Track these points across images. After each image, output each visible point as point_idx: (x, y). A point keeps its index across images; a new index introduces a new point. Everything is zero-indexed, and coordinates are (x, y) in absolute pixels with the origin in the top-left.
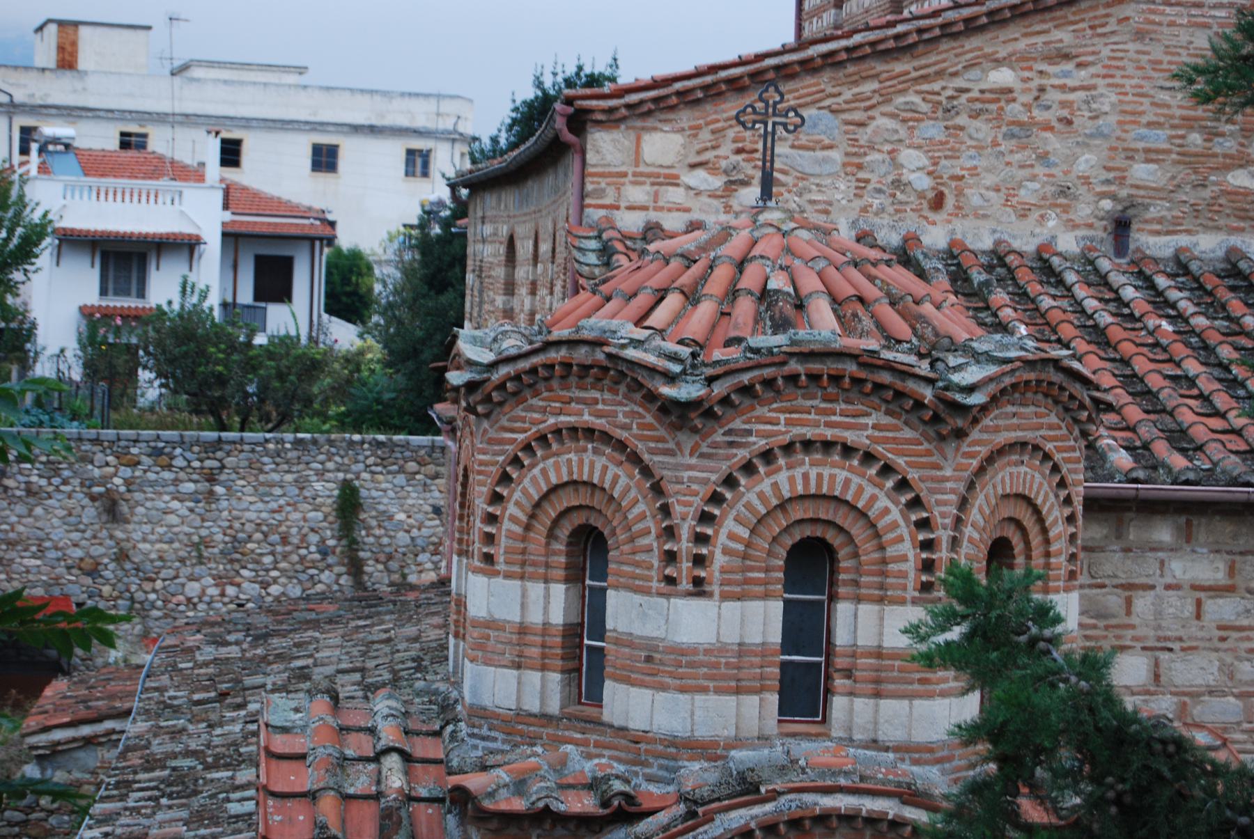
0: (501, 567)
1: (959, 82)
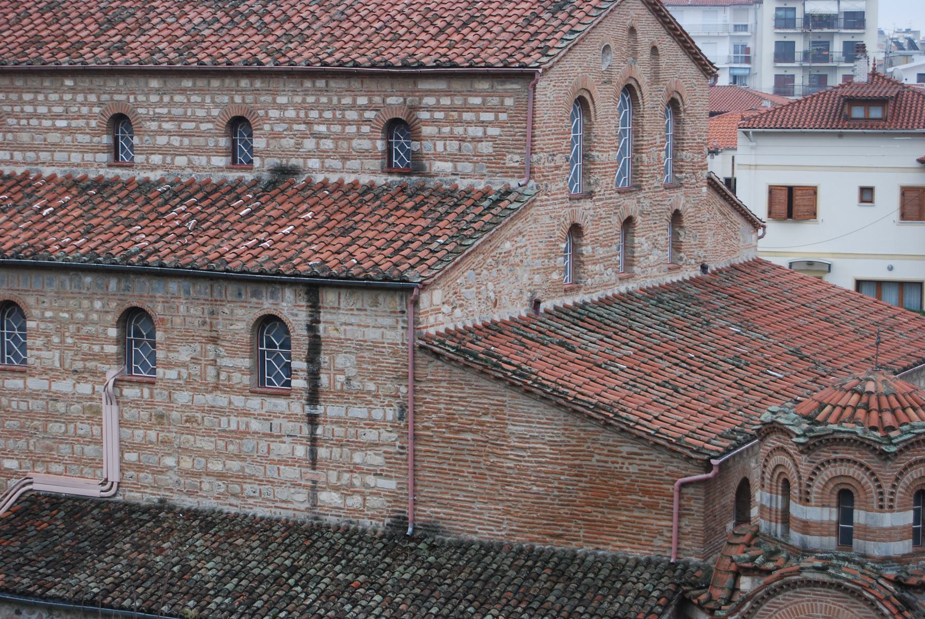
0: (896, 508)
1: (499, 251)
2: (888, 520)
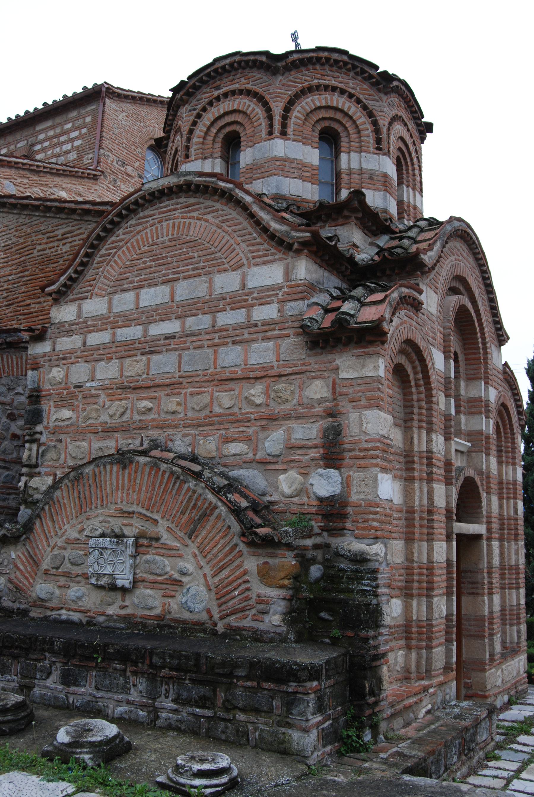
2: (279, 147)
